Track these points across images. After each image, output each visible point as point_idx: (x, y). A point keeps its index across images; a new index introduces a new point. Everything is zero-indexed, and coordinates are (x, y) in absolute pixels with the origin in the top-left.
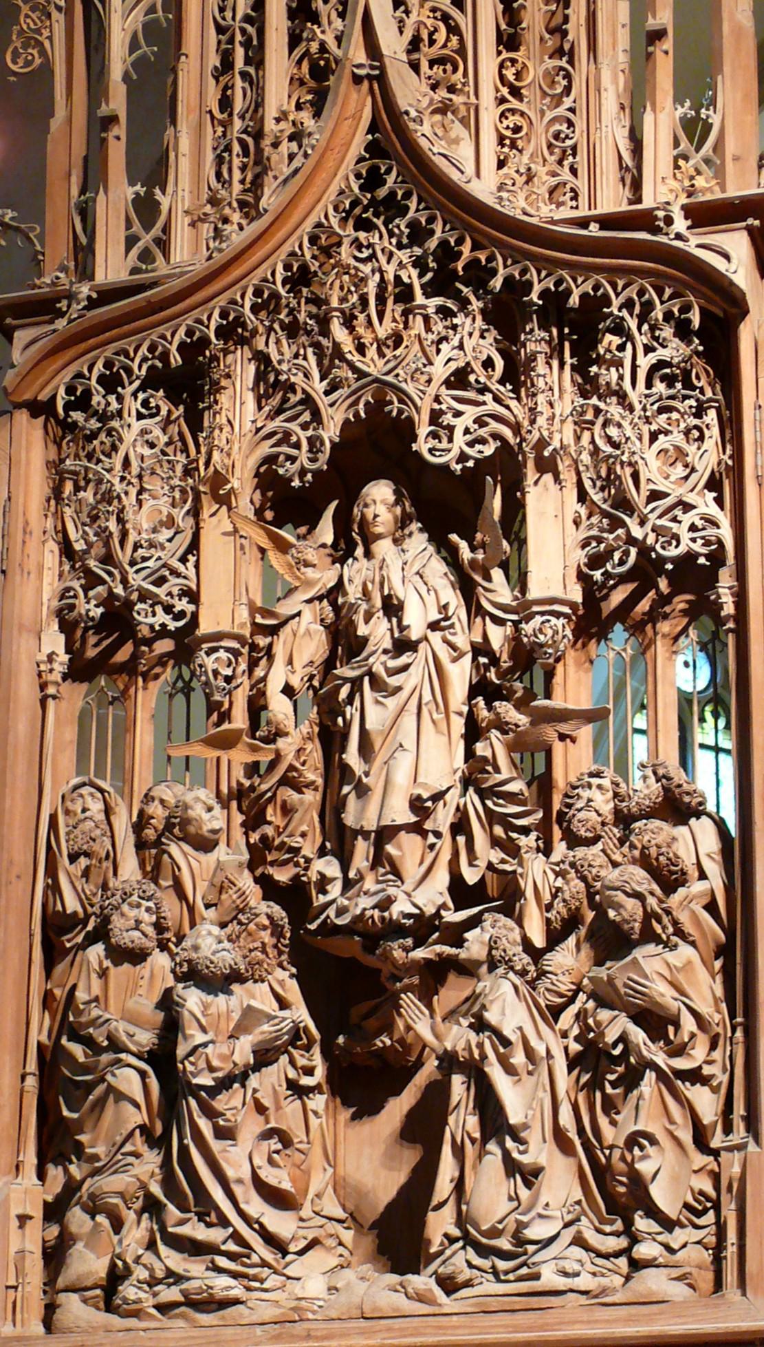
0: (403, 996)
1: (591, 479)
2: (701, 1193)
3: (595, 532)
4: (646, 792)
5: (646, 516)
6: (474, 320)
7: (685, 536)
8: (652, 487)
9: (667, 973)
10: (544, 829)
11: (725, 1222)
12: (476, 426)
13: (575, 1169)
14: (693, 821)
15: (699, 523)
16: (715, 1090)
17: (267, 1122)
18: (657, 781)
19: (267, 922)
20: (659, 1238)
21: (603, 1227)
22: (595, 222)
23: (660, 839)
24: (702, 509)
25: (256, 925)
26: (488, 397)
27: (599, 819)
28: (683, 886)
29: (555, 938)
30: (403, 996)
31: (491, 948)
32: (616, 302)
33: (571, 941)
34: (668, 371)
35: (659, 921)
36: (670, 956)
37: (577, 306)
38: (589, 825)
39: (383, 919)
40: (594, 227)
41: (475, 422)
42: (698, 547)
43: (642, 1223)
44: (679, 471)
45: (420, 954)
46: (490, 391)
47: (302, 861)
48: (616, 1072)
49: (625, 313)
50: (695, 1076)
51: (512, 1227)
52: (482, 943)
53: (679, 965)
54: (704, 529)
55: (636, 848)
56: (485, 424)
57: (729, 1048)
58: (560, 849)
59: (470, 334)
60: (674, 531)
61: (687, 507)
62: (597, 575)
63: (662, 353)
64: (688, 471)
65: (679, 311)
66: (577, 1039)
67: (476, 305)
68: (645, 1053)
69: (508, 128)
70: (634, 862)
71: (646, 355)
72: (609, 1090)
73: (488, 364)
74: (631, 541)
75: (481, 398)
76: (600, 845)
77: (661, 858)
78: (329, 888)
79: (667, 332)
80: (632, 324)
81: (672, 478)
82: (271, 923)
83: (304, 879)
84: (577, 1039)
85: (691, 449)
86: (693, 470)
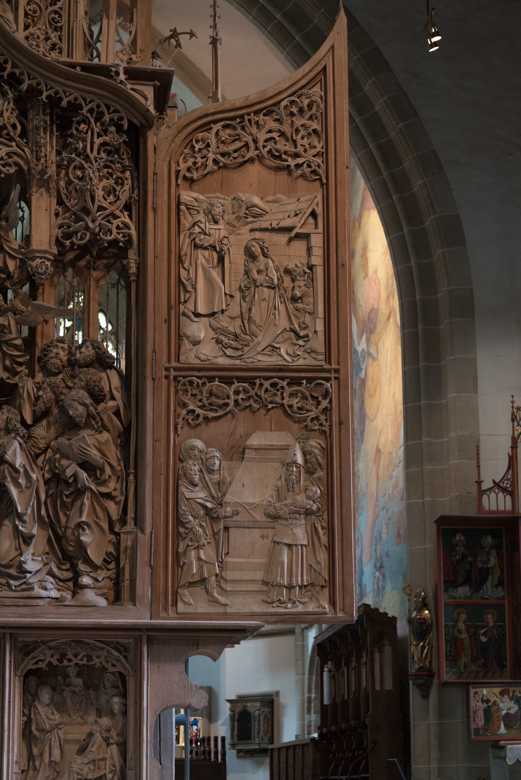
1: (65, 194)
2: (111, 553)
3: (66, 221)
4: (88, 354)
5: (96, 217)
6: (9, 103)
7: (115, 231)
8: (100, 204)
9: (97, 445)
10: (30, 365)
11: (123, 568)
12: (7, 157)
13: (47, 537)
14: (108, 371)
15: (121, 226)
16: (117, 503)
18: (93, 349)
20: (91, 574)
21: (61, 566)
22: (79, 66)
23: (95, 378)
24: (123, 219)
26: (14, 144)
27: (61, 364)
28: (103, 402)
29: (36, 420)
31: (7, 423)
32: (86, 109)
33: (44, 422)
34: (108, 148)
35: (94, 419)
36: (98, 436)
37: (65, 106)
38: (57, 365)
40: (78, 69)
41: (6, 154)
42: (120, 237)
43: (82, 567)
44: (111, 198)
46: (15, 141)
48: (70, 490)
49: (88, 115)
50: (108, 496)
51: (17, 563)
53: (103, 441)
54: (123, 229)
55: (83, 381)
56: (12, 157)
57: (124, 484)
58: (39, 377)
59: (7, 110)
60: (110, 227)
61: (116, 217)
62: (68, 243)
63: (107, 139)
64: (116, 199)
65: (117, 119)
66: (48, 471)
67: (10, 96)
68: (87, 483)
69: (30, 10)
70: (82, 388)
71: (98, 138)
72: (65, 499)
73: (14, 127)
74: (87, 228)
75: (9, 143)
76: (61, 376)
77: (96, 388)
79: (113, 129)
80: (92, 121)
81: (108, 201)
84: (48, 471)
85: (118, 188)
86: (118, 199)
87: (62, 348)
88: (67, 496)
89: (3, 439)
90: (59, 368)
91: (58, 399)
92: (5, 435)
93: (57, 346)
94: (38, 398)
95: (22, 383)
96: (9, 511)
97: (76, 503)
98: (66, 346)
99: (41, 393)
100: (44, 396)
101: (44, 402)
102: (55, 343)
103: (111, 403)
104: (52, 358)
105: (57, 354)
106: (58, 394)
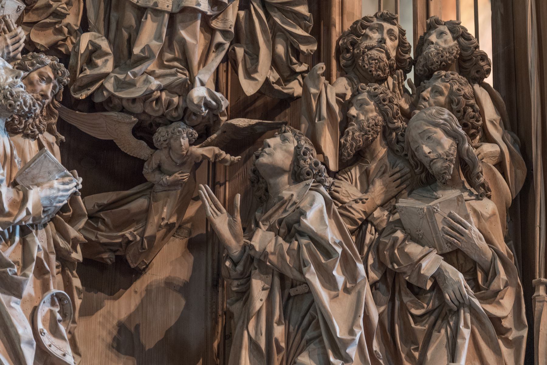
0: (202, 186)
17: (45, 288)
19: (52, 76)
25: (41, 75)
30: (202, 186)
39: (170, 103)
45: (198, 150)
47: (66, 30)
48: (423, 308)
52: (287, 151)
78: (99, 62)
82: (55, 78)
83: (63, 50)
84: (373, 266)
87: (390, 32)
88: (417, 319)
89: (289, 190)
90: (385, 70)
91: (390, 125)
92: (289, 183)
93: (380, 29)
94: (347, 120)
95: (317, 87)
96: (307, 336)
97: (435, 334)
98: (396, 29)
99: (353, 111)
100: (362, 117)
101: (361, 129)
102: (375, 21)
103: (487, 148)
104: (371, 48)
105: (382, 41)
106: (390, 115)
